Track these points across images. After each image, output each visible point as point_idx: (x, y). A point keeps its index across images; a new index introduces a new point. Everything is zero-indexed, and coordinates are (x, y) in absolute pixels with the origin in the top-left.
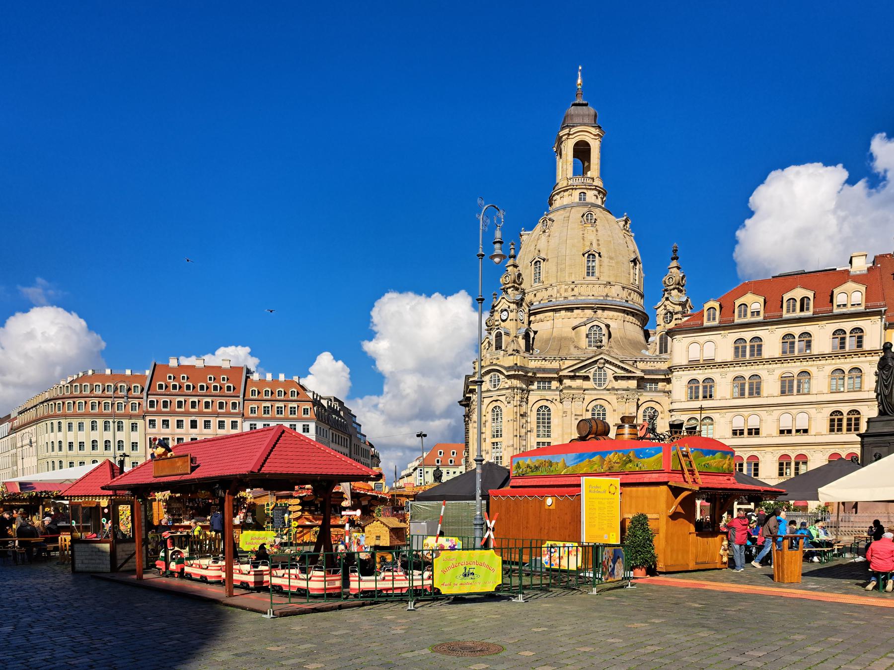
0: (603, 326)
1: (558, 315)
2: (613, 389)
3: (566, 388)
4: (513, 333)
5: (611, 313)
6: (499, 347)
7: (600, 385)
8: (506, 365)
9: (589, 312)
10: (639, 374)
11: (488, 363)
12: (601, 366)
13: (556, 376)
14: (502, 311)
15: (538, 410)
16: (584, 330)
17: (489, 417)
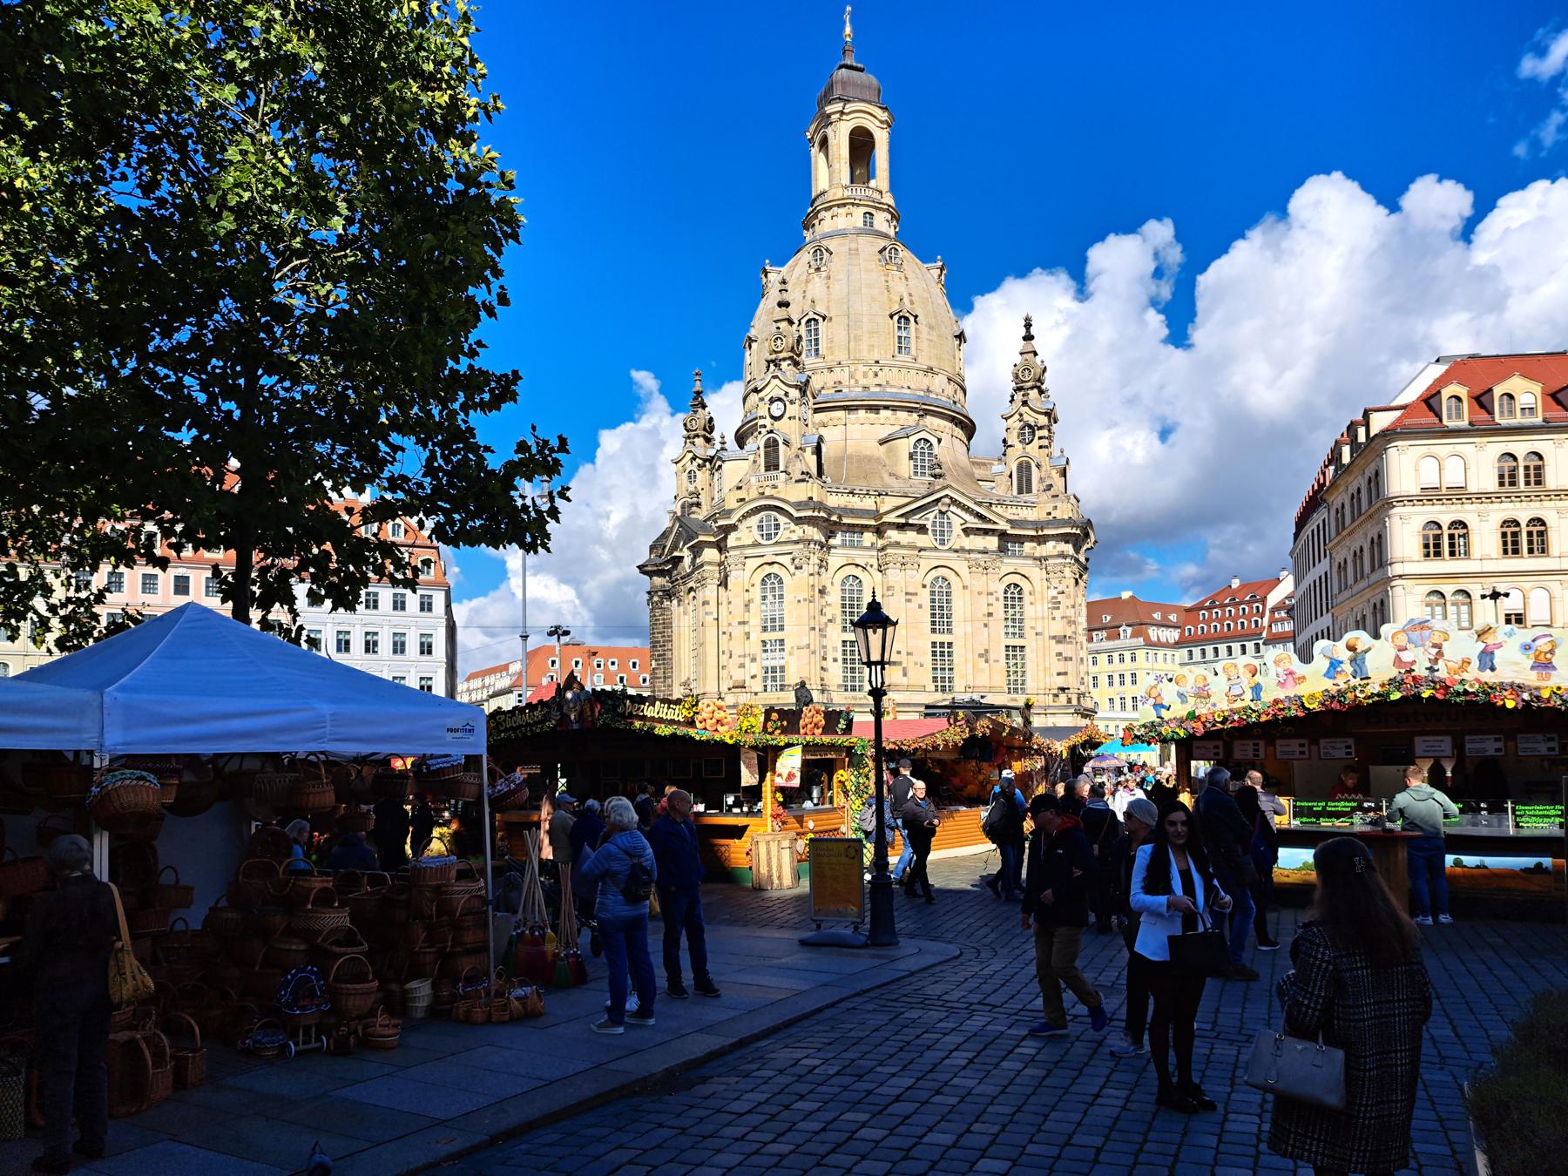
0: (934, 441)
1: (853, 416)
2: (963, 550)
3: (891, 545)
6: (772, 465)
7: (942, 542)
8: (793, 500)
9: (902, 415)
10: (1003, 526)
11: (754, 494)
13: (872, 522)
14: (772, 401)
15: (843, 583)
16: (905, 446)
17: (756, 593)
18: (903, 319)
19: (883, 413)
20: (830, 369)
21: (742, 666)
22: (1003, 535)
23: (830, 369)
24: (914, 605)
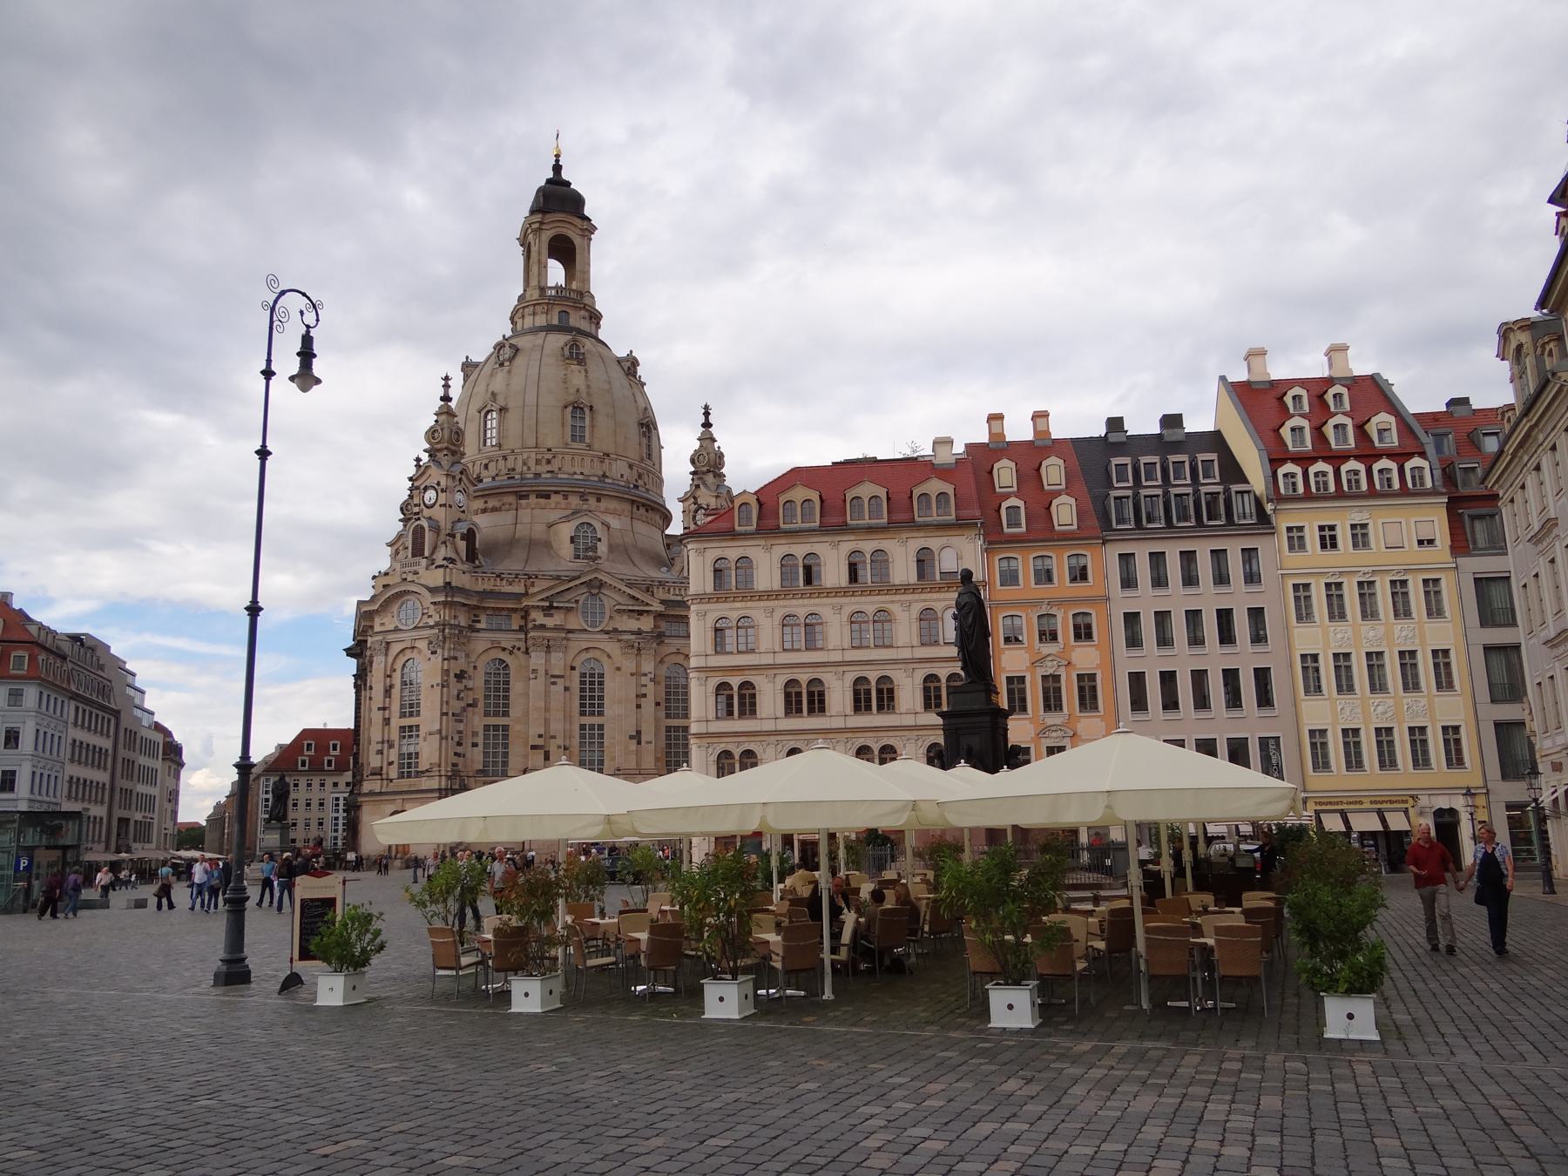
0: (597, 525)
2: (615, 630)
4: (445, 527)
5: (613, 505)
9: (574, 501)
10: (657, 607)
12: (595, 591)
14: (426, 489)
16: (567, 530)
18: (577, 408)
19: (555, 498)
20: (505, 458)
21: (380, 752)
22: (659, 616)
23: (505, 458)
24: (559, 688)
